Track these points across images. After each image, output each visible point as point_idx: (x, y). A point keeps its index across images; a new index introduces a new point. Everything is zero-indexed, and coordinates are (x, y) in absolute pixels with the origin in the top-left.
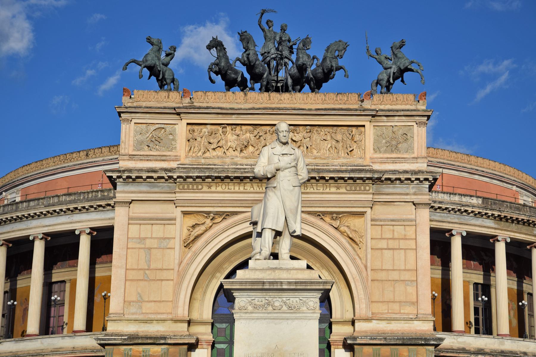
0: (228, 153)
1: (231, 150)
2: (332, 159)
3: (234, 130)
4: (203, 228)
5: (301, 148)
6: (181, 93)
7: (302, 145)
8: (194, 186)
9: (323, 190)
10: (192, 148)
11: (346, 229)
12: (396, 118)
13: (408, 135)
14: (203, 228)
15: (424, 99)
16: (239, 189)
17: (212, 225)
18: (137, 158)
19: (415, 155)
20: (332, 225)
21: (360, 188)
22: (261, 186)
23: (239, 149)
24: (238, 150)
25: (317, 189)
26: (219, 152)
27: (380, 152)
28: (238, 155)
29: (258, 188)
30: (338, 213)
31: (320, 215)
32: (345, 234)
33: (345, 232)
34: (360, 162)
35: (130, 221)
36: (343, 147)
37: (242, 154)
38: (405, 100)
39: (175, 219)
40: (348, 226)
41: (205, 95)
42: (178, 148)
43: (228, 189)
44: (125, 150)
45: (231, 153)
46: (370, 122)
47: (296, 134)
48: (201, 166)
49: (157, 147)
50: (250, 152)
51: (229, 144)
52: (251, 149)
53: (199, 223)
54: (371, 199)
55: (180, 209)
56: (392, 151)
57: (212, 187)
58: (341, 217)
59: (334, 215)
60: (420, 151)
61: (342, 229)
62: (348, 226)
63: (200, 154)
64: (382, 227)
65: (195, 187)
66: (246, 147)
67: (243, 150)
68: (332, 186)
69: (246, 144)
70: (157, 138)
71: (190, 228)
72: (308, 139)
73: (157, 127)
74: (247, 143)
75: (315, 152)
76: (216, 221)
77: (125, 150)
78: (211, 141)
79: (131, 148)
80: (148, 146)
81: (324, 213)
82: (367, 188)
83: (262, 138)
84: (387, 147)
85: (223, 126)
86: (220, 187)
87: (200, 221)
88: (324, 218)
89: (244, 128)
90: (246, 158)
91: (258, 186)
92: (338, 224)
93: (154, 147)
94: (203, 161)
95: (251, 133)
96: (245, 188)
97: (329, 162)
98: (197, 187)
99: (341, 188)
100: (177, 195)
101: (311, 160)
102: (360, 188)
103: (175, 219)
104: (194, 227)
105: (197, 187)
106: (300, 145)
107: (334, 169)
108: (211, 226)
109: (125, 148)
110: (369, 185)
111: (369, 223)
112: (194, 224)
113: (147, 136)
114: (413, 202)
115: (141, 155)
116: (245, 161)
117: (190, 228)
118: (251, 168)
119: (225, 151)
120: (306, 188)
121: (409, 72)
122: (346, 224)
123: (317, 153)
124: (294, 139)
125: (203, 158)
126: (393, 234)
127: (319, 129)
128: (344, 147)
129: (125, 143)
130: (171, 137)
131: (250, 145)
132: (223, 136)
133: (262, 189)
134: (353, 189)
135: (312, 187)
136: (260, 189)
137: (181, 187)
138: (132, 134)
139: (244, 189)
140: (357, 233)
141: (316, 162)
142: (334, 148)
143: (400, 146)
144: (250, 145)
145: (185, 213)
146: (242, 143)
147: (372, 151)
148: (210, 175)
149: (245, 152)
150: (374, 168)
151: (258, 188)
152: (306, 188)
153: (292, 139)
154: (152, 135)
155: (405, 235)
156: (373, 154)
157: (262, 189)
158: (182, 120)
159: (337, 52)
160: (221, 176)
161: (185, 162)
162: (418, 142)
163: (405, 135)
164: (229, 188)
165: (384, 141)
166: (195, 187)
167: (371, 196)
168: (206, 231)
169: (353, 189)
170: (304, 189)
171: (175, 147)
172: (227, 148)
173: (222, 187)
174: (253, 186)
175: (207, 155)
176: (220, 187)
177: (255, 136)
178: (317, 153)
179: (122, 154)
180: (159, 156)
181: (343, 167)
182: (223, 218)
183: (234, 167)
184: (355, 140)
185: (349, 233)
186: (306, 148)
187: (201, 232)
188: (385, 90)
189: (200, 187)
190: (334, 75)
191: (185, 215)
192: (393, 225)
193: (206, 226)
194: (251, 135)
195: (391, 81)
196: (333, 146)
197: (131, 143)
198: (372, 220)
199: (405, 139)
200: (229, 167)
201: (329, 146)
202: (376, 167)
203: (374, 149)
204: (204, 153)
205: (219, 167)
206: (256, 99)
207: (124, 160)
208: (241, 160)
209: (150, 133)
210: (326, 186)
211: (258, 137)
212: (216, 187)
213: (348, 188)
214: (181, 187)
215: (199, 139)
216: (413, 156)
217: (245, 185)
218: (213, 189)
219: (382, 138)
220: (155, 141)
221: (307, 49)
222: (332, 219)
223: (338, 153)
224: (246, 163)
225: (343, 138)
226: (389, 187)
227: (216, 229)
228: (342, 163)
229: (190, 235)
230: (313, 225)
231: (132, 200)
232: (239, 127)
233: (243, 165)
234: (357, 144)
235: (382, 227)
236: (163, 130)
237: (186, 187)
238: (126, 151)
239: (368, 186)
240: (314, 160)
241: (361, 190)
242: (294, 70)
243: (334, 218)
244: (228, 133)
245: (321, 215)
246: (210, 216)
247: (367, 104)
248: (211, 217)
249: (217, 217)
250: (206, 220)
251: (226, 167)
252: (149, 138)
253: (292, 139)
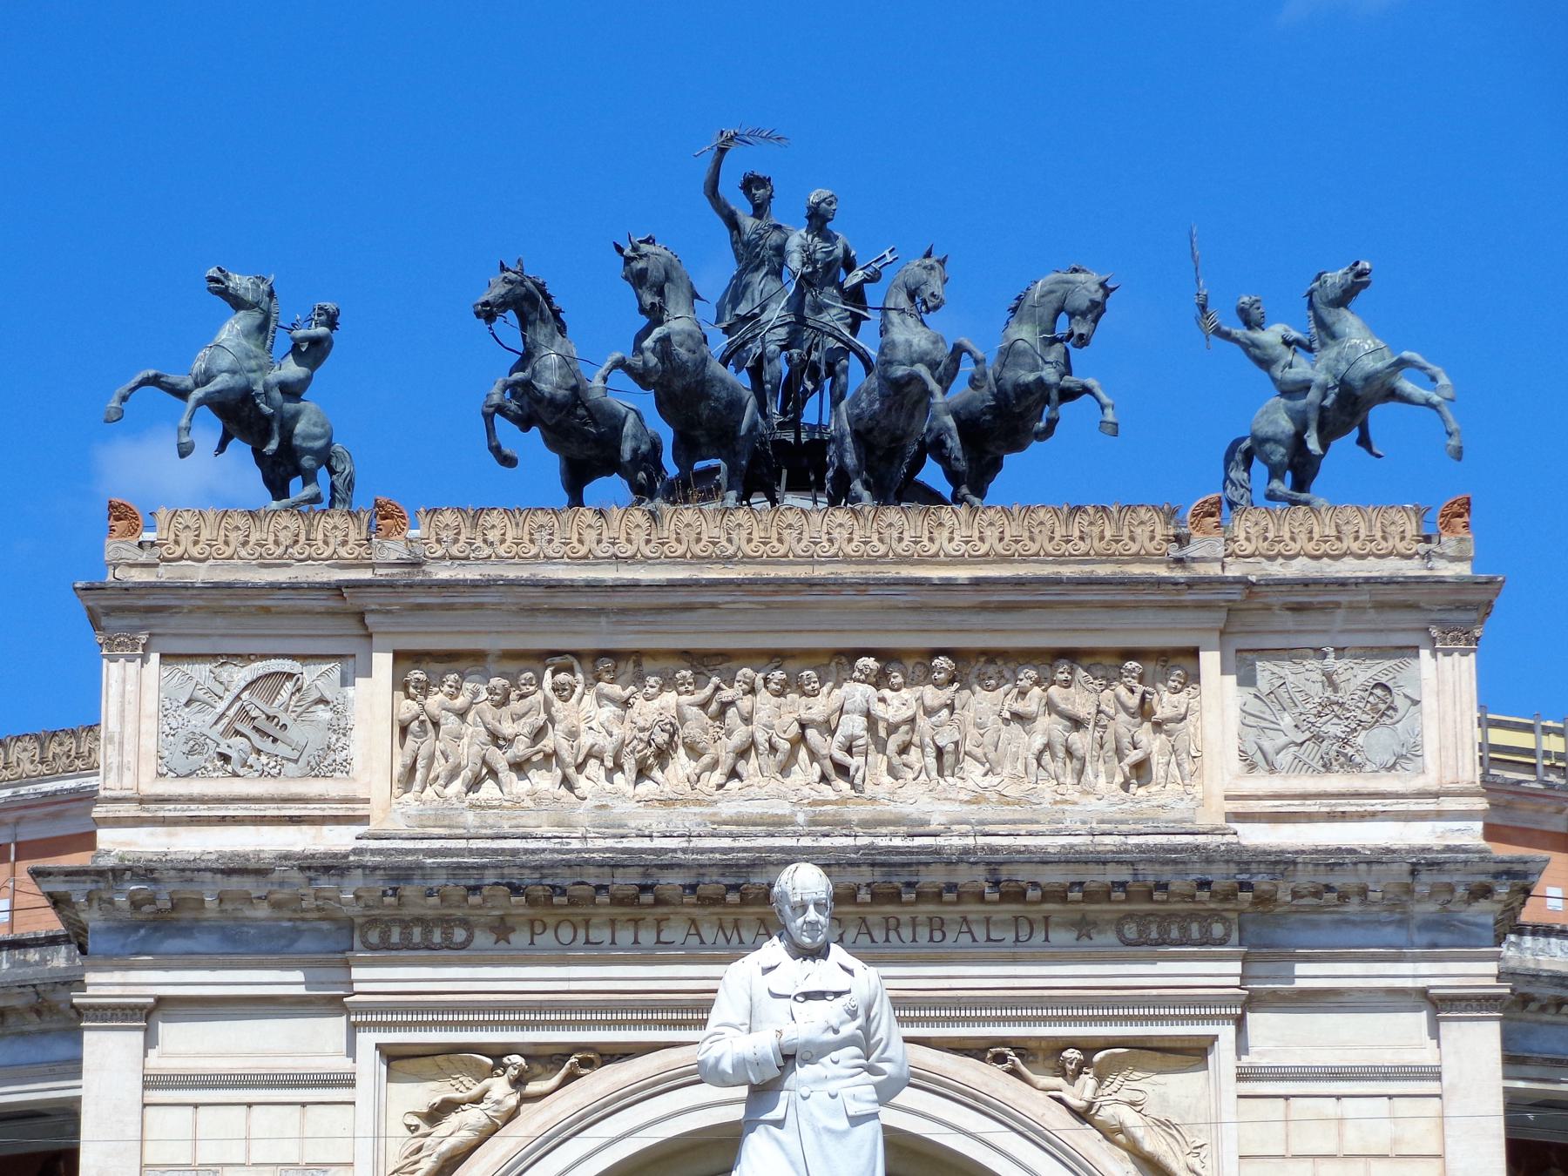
0: (582, 782)
1: (593, 766)
2: (1056, 802)
3: (608, 677)
4: (473, 1117)
5: (914, 755)
6: (365, 518)
7: (916, 739)
8: (431, 931)
9: (1017, 940)
10: (420, 764)
11: (1129, 1117)
12: (1340, 614)
13: (1394, 691)
14: (473, 1117)
15: (1460, 529)
16: (636, 942)
17: (518, 1106)
18: (175, 810)
19: (1429, 781)
20: (1060, 1100)
21: (1184, 930)
22: (736, 926)
23: (629, 764)
24: (626, 767)
25: (989, 939)
26: (544, 781)
27: (1272, 769)
28: (629, 789)
29: (720, 933)
30: (1089, 1047)
31: (1000, 1059)
32: (1120, 1137)
33: (1121, 1132)
34: (1181, 809)
35: (147, 1093)
36: (1102, 747)
37: (646, 787)
38: (1379, 535)
39: (349, 1082)
40: (1132, 1104)
41: (475, 526)
42: (357, 764)
43: (587, 942)
44: (120, 775)
45: (591, 781)
46: (1222, 633)
47: (886, 693)
48: (462, 844)
49: (264, 759)
50: (681, 774)
51: (586, 740)
52: (681, 763)
53: (457, 1095)
54: (1236, 981)
55: (367, 1041)
56: (1327, 767)
57: (512, 937)
58: (1102, 1060)
59: (1067, 1054)
60: (1451, 762)
61: (1109, 1113)
62: (1132, 1104)
63: (457, 786)
64: (1287, 1106)
65: (437, 937)
66: (663, 755)
67: (651, 768)
68: (1060, 925)
69: (661, 738)
70: (262, 723)
71: (415, 1121)
72: (945, 712)
73: (261, 672)
74: (666, 736)
75: (974, 771)
76: (533, 1087)
77: (120, 775)
78: (507, 728)
79: (149, 768)
80: (220, 754)
81: (1024, 1049)
82: (1218, 930)
83: (732, 712)
84: (1302, 744)
85: (557, 660)
86: (550, 934)
87: (462, 1088)
88: (1023, 1069)
89: (647, 665)
90: (667, 803)
91: (721, 927)
92: (1088, 1095)
93: (252, 759)
94: (470, 818)
95: (682, 689)
96: (662, 939)
97: (1041, 817)
98: (447, 936)
99: (1099, 932)
100: (357, 973)
101: (956, 807)
102: (1184, 930)
103: (349, 1082)
104: (436, 1114)
105: (447, 936)
106: (907, 738)
107: (1063, 846)
108: (512, 1115)
109: (121, 767)
110: (1224, 914)
111: (1232, 1087)
112: (437, 1099)
113: (219, 710)
114: (1424, 992)
115: (191, 800)
116: (655, 819)
117: (415, 1121)
118: (684, 851)
119: (571, 771)
120: (938, 936)
121: (1393, 406)
122: (1125, 1095)
123: (986, 774)
124: (879, 709)
125: (472, 806)
126: (1340, 1135)
127: (991, 670)
128: (1106, 747)
129: (121, 744)
130: (323, 714)
131: (680, 742)
132: (558, 704)
133: (741, 942)
134: (1154, 935)
135: (965, 929)
136: (728, 941)
137: (374, 937)
138: (151, 705)
139: (658, 942)
140: (1175, 1132)
141: (983, 816)
142: (1061, 754)
143: (1360, 739)
144: (680, 742)
145: (396, 1059)
146: (645, 736)
147: (1236, 765)
148: (504, 881)
149: (656, 773)
150: (1244, 842)
151: (721, 939)
152: (938, 936)
153: (868, 714)
154: (242, 708)
155: (1395, 1141)
156: (1239, 777)
157: (741, 942)
158: (370, 636)
159: (1063, 317)
160: (553, 887)
161: (389, 826)
162: (1442, 720)
163: (1378, 692)
164: (592, 939)
165: (1287, 720)
166: (437, 937)
167: (1236, 967)
168: (488, 1132)
169: (1154, 935)
170: (931, 939)
171: (347, 761)
172: (580, 760)
173: (559, 931)
174: (697, 930)
175: (488, 790)
176: (550, 934)
177: (704, 706)
178: (986, 774)
179: (108, 793)
180: (272, 800)
181: (1107, 840)
182: (563, 1071)
183: (610, 843)
184: (1161, 713)
185: (1139, 1133)
186: (931, 751)
187: (466, 1135)
188: (1283, 487)
189: (459, 935)
190: (1052, 423)
191: (393, 1063)
192: (1338, 1097)
193: (490, 1113)
194: (685, 698)
195: (1313, 444)
196: (1059, 747)
197: (149, 744)
198: (1242, 1077)
199: (1383, 707)
200: (590, 845)
201: (1038, 741)
202: (1256, 836)
203: (1243, 755)
204: (475, 784)
205: (542, 844)
206: (705, 537)
207: (118, 822)
208: (641, 810)
209: (229, 697)
210: (1031, 923)
211: (714, 707)
212: (533, 934)
213: (1131, 931)
214: (374, 937)
215: (450, 723)
216: (1418, 783)
217: (664, 923)
218: (520, 938)
219: (1279, 707)
220: (255, 737)
221: (928, 311)
222: (1063, 1073)
223: (1080, 773)
224: (663, 827)
225: (1103, 707)
226: (1315, 925)
227: (535, 1120)
228: (1100, 817)
229: (419, 1150)
230: (976, 1098)
231: (161, 1001)
232: (631, 666)
233: (650, 836)
234: (1169, 734)
235: (1287, 1106)
236: (289, 686)
237: (395, 937)
238: (128, 780)
239: (1224, 921)
240: (974, 807)
241: (1189, 938)
242: (871, 403)
243: (1068, 1065)
244: (579, 689)
245: (1011, 1055)
246: (505, 1068)
247: (1206, 549)
248: (510, 1068)
249: (537, 1069)
250: (487, 1082)
251: (576, 844)
252: (225, 721)
253: (868, 714)
